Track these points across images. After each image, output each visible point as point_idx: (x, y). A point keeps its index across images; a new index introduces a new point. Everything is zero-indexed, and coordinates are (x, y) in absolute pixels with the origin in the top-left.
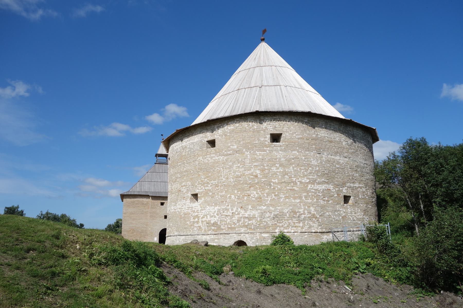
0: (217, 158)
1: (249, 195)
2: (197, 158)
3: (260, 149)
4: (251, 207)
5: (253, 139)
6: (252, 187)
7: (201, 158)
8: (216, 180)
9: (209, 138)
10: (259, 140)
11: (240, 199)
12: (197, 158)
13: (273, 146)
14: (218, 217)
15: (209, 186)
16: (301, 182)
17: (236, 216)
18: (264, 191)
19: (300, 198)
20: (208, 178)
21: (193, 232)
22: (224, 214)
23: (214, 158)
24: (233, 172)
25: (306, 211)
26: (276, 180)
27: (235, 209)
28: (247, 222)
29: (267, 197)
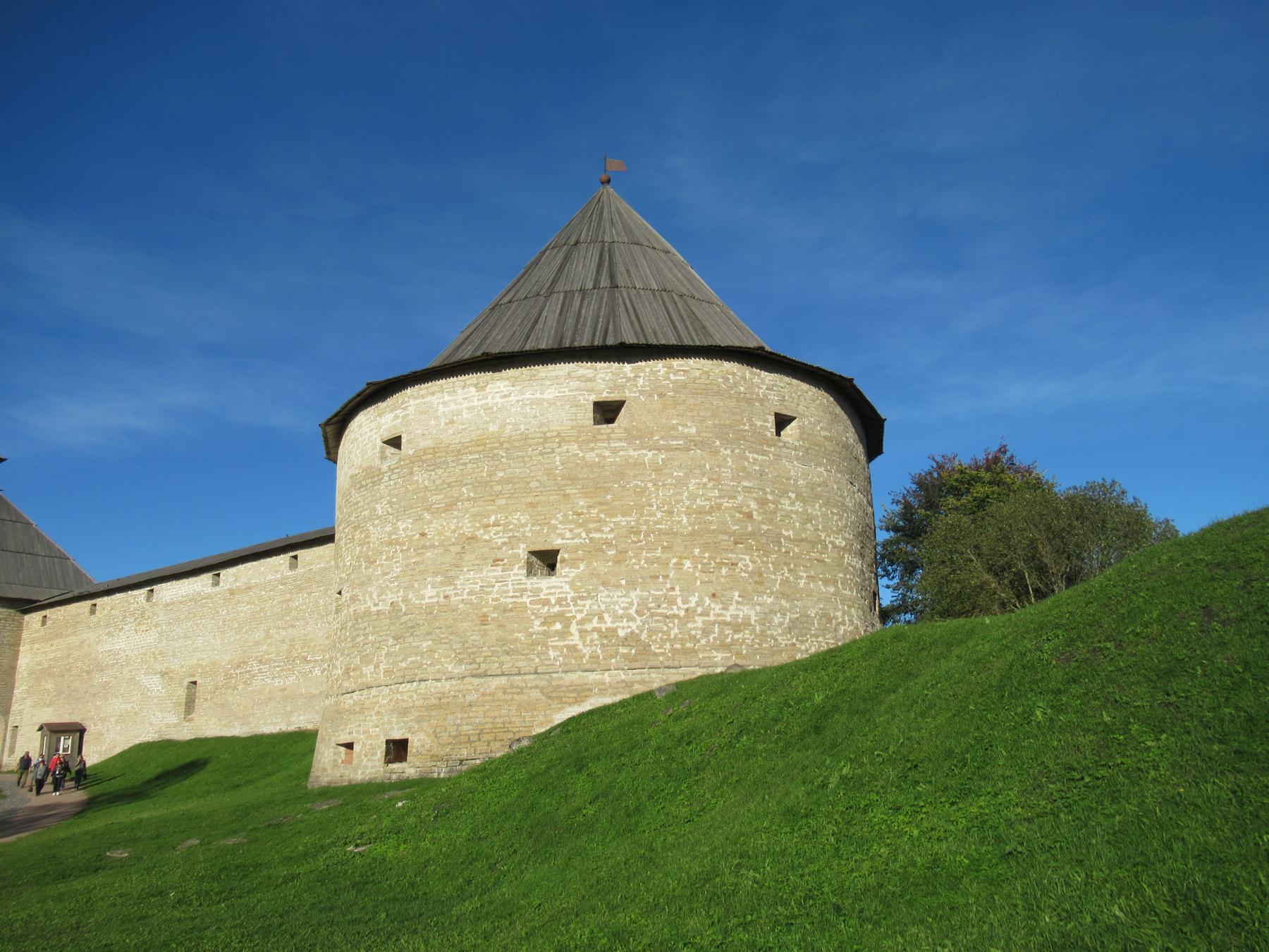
0: (632, 453)
1: (732, 564)
2: (556, 445)
3: (754, 446)
4: (739, 596)
5: (738, 418)
6: (742, 544)
7: (574, 447)
8: (630, 515)
9: (605, 394)
10: (750, 420)
11: (710, 572)
12: (559, 447)
13: (781, 444)
14: (641, 621)
15: (609, 529)
16: (834, 546)
17: (699, 622)
18: (768, 557)
19: (835, 583)
20: (603, 507)
21: (543, 665)
22: (659, 611)
23: (622, 453)
24: (688, 498)
25: (846, 618)
26: (791, 532)
27: (694, 600)
28: (730, 636)
29: (775, 574)
